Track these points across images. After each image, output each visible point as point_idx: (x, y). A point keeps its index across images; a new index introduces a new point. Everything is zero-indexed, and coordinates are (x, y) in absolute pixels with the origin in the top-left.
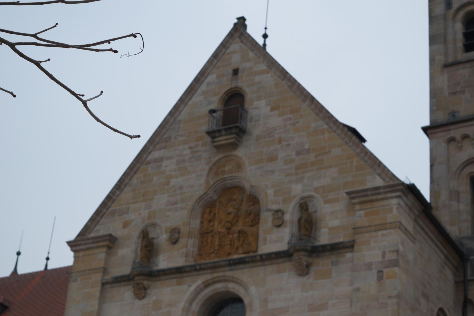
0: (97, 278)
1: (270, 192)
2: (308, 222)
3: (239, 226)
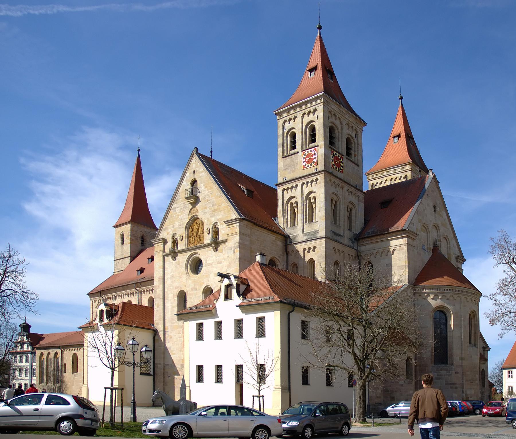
0: (161, 254)
1: (206, 220)
2: (216, 233)
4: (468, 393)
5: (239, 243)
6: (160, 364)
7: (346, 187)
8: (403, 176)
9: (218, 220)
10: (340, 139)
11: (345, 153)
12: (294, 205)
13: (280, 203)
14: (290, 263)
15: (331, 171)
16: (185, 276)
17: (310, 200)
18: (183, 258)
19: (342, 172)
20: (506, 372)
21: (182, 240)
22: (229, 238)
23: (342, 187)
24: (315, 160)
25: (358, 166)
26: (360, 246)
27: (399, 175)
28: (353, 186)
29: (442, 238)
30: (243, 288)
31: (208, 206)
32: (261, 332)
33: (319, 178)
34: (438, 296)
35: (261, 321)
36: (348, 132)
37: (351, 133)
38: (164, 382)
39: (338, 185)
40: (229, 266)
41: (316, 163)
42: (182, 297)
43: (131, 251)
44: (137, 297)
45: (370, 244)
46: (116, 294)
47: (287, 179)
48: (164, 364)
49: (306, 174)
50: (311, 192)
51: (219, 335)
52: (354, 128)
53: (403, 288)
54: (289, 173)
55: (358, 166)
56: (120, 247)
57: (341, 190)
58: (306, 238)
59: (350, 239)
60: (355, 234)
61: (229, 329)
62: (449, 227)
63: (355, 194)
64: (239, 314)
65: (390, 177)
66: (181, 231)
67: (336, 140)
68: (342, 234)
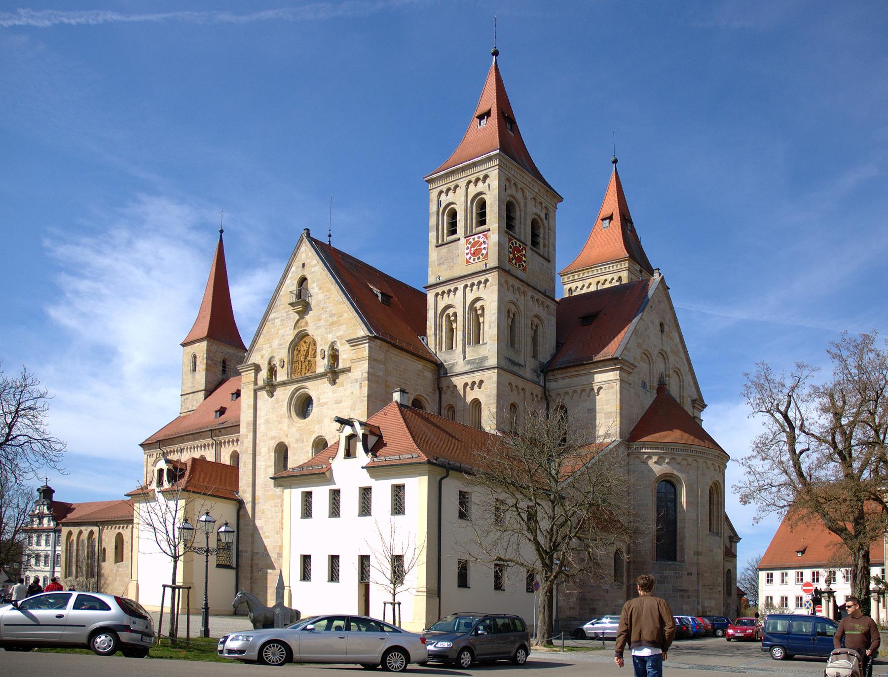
0: (252, 387)
2: (335, 357)
3: (308, 358)
4: (706, 604)
5: (369, 373)
6: (246, 552)
7: (530, 293)
8: (616, 278)
9: (337, 338)
10: (523, 221)
11: (529, 242)
12: (452, 318)
13: (431, 314)
14: (444, 404)
15: (507, 268)
16: (286, 420)
17: (476, 311)
18: (283, 394)
19: (524, 269)
20: (763, 575)
21: (283, 367)
22: (353, 366)
23: (524, 293)
24: (484, 252)
25: (549, 261)
26: (550, 381)
27: (609, 277)
28: (540, 292)
29: (671, 371)
30: (372, 440)
31: (323, 317)
32: (398, 508)
33: (490, 279)
34: (664, 459)
35: (398, 490)
36: (535, 210)
37: (538, 212)
38: (251, 578)
39: (518, 289)
40: (353, 408)
41: (486, 256)
42: (282, 452)
43: (207, 382)
44: (213, 451)
45: (563, 378)
46: (182, 445)
47: (442, 279)
48: (252, 551)
49: (470, 272)
50: (478, 299)
51: (335, 511)
52: (544, 205)
53: (612, 446)
54: (446, 270)
55: (549, 261)
56: (190, 376)
57: (523, 297)
58: (468, 368)
59: (535, 371)
60: (541, 364)
61: (350, 502)
62: (682, 355)
63: (543, 303)
64: (366, 480)
65: (597, 279)
66: (282, 354)
67: (517, 222)
68: (522, 363)
